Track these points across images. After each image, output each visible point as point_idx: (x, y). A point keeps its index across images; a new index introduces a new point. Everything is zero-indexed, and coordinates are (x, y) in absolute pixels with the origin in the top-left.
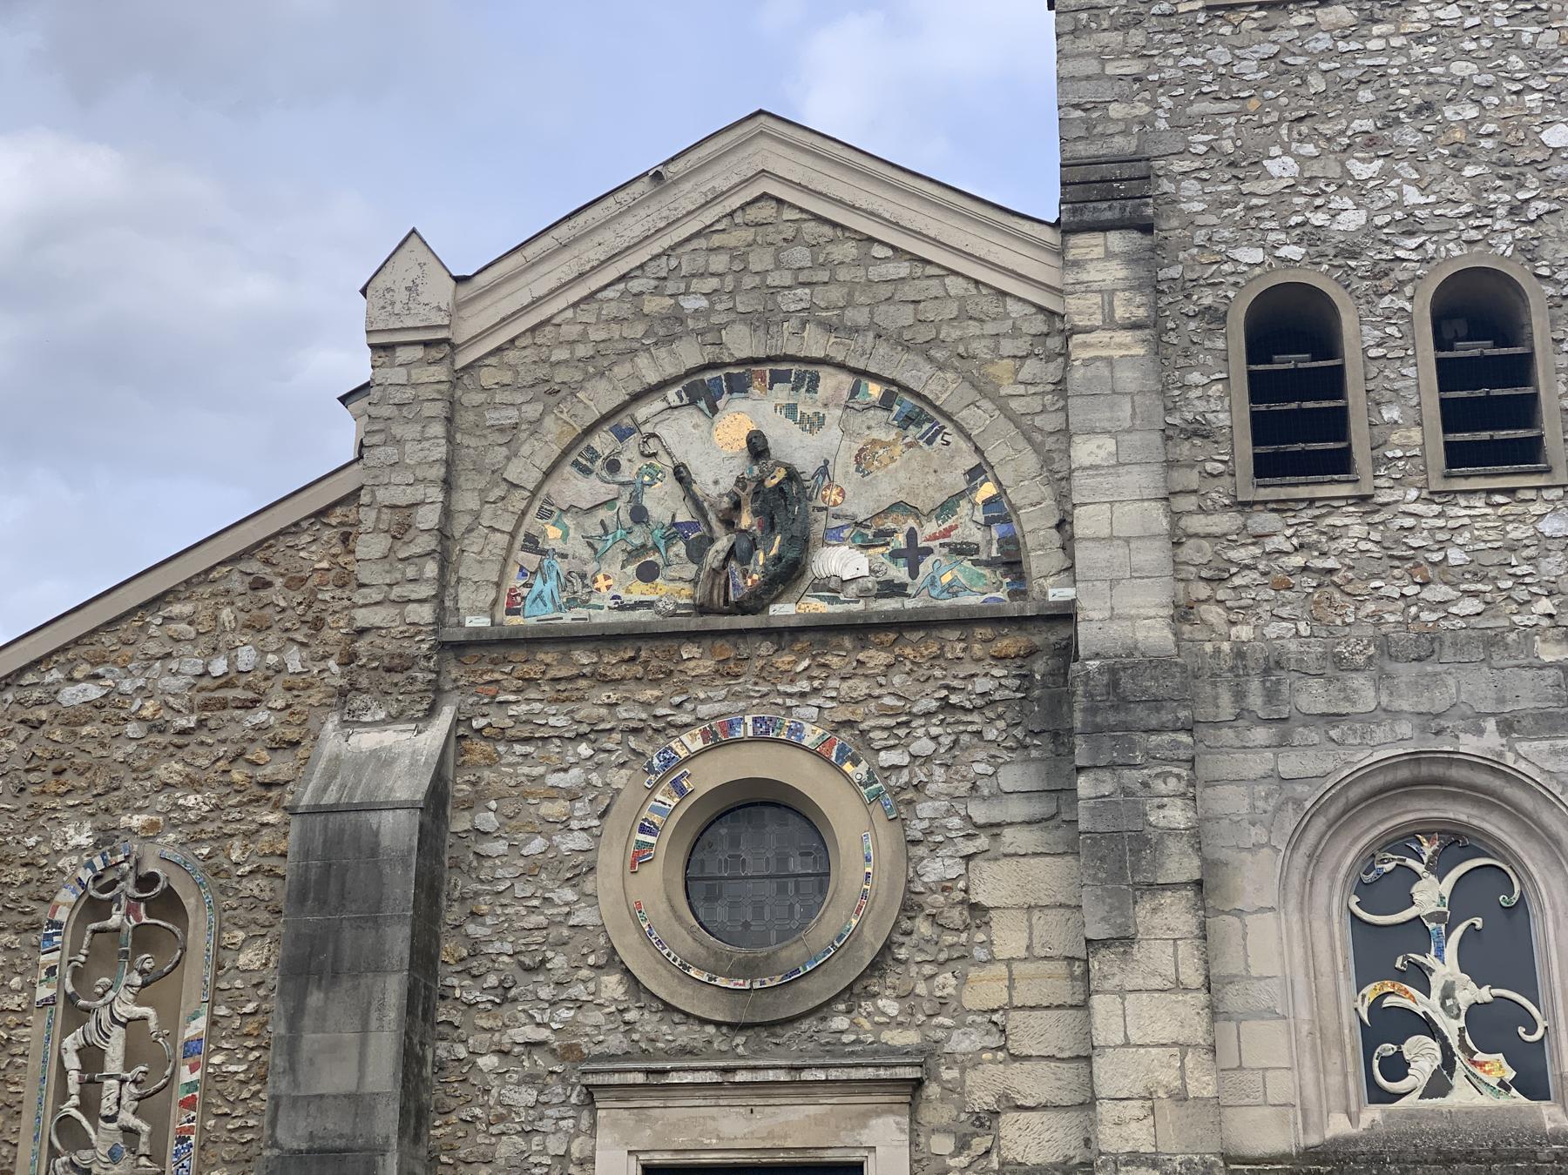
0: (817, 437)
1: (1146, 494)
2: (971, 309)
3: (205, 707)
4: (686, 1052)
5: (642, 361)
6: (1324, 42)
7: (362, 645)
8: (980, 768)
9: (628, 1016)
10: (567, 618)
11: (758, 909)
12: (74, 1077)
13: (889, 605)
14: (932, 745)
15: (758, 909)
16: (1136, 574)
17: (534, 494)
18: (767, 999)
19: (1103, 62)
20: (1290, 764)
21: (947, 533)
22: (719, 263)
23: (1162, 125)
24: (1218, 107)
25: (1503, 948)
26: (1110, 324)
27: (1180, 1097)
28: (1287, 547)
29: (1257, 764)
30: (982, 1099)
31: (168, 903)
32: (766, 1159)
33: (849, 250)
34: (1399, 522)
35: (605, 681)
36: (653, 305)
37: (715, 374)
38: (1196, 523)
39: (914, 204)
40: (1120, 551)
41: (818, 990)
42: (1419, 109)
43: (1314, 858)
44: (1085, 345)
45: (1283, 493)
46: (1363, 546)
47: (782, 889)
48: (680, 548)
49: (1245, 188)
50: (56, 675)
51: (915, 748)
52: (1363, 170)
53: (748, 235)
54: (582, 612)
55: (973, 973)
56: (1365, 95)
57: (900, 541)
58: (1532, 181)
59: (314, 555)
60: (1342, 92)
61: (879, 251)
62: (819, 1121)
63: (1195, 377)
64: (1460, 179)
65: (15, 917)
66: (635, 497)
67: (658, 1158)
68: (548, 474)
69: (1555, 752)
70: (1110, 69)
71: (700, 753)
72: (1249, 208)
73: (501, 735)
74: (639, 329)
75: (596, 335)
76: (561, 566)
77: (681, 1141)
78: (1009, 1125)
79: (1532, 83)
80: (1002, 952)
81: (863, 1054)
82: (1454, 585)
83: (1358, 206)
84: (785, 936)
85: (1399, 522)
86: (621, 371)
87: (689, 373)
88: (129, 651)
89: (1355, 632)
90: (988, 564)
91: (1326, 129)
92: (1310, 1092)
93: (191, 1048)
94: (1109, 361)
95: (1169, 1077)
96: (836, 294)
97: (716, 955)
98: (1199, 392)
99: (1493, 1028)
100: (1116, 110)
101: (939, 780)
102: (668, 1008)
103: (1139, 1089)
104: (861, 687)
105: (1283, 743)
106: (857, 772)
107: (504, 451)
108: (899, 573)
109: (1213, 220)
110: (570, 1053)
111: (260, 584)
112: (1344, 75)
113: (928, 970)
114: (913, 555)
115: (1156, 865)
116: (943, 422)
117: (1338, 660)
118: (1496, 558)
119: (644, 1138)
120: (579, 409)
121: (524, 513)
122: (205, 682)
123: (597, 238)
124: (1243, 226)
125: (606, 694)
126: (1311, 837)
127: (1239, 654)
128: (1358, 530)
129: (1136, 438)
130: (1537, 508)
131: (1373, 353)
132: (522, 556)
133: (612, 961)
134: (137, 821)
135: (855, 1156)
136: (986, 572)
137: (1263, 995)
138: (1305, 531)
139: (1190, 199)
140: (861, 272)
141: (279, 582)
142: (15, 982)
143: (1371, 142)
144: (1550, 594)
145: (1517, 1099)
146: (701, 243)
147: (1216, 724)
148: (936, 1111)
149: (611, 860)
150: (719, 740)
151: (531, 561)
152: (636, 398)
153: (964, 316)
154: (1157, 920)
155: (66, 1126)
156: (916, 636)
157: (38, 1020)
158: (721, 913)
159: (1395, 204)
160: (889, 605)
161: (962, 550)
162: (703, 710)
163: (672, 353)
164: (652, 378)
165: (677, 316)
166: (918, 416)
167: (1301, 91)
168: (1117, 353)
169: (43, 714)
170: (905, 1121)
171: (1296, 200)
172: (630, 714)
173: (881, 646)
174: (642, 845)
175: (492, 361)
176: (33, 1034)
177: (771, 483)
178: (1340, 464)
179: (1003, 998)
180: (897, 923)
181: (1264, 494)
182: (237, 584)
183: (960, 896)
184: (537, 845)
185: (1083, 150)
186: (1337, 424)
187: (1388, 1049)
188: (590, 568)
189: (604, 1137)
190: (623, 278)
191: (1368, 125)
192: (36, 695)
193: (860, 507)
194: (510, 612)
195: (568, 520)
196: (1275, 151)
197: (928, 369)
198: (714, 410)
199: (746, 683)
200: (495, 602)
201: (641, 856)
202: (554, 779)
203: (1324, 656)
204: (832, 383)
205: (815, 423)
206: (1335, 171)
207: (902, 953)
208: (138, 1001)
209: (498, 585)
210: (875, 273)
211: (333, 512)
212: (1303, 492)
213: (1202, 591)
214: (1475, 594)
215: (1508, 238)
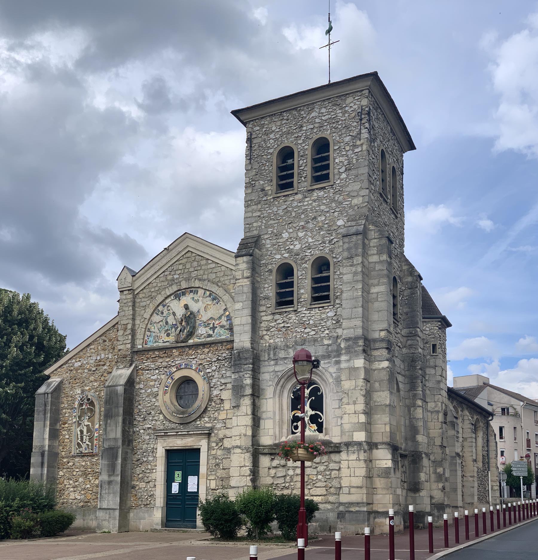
0: (197, 304)
1: (248, 315)
2: (226, 273)
3: (97, 366)
4: (173, 429)
5: (167, 290)
6: (295, 204)
7: (119, 353)
8: (224, 372)
9: (164, 422)
10: (155, 345)
11: (188, 402)
12: (79, 435)
13: (209, 339)
14: (215, 368)
15: (188, 402)
16: (245, 332)
17: (149, 320)
18: (186, 419)
19: (253, 213)
20: (277, 368)
21: (220, 323)
22: (181, 267)
23: (263, 227)
24: (274, 222)
25: (318, 404)
26: (243, 278)
27: (245, 435)
28: (281, 322)
29: (271, 369)
30: (221, 436)
31: (92, 403)
32: (184, 448)
33: (204, 262)
34: (301, 315)
35: (160, 357)
36: (169, 277)
37: (180, 292)
38: (264, 318)
39: (214, 251)
40: (242, 327)
41: (194, 417)
42: (313, 219)
43: (283, 387)
44: (238, 283)
45: (280, 311)
46: (295, 321)
47: (192, 397)
48: (174, 329)
49: (278, 241)
50: (74, 361)
51: (213, 368)
52: (301, 234)
53: (185, 260)
54: (157, 344)
55: (221, 412)
56: (303, 216)
57: (211, 326)
58: (334, 234)
59: (112, 335)
60: (298, 216)
61: (210, 262)
62: (193, 441)
63: (266, 286)
64: (320, 235)
65: (70, 407)
66: (166, 319)
67: (167, 448)
68: (151, 315)
69: (325, 363)
70: (254, 215)
71: (176, 371)
72: (279, 246)
73: (143, 369)
74: (167, 283)
75: (159, 285)
76: (154, 334)
77: (171, 445)
78: (225, 441)
79: (336, 210)
80: (225, 408)
81: (202, 428)
82: (310, 328)
83: (299, 243)
84: (189, 407)
85: (301, 315)
86: (163, 293)
87: (175, 292)
88: (85, 355)
89: (291, 340)
90: (226, 329)
91: (295, 225)
92: (277, 433)
93: (96, 430)
94: (242, 286)
95: (243, 432)
96: (201, 272)
97: (178, 410)
98: (266, 289)
99: (314, 419)
100: (255, 225)
101: (216, 375)
102: (170, 421)
103: (238, 434)
104: (203, 356)
105: (276, 364)
106: (202, 374)
107: (144, 311)
108: (211, 332)
109: (272, 249)
110: (154, 429)
111: (105, 341)
112: (299, 211)
113: (213, 412)
114: (213, 328)
115: (244, 391)
116: (220, 299)
117: (288, 347)
118: (319, 322)
119: (165, 445)
120: (156, 301)
121: (147, 324)
122: (97, 361)
123: (158, 264)
124: (277, 250)
125: (161, 360)
126: (281, 383)
127: (269, 346)
128: (294, 318)
129: (246, 303)
130: (327, 311)
131: (300, 278)
132: (147, 333)
133: (161, 413)
134: (87, 388)
135: (199, 447)
136: (226, 331)
137: (270, 415)
138: (284, 318)
139: (268, 244)
140: (206, 267)
141: (107, 340)
142: (70, 419)
143: (303, 227)
144: (328, 329)
145: (317, 433)
146: (177, 263)
147: (265, 361)
148: (213, 439)
149: (161, 393)
150: (178, 369)
151: (148, 333)
152: (166, 298)
153: (224, 275)
154: (244, 402)
155: (78, 444)
156: (213, 345)
157: (74, 425)
158: (182, 402)
159: (307, 242)
160: (209, 339)
161: (222, 327)
162: (177, 362)
163: (172, 288)
164: (168, 294)
165: (173, 280)
166: (215, 298)
167: (291, 216)
168: (244, 284)
169: (72, 368)
170: (207, 441)
171: (288, 243)
172: (165, 364)
173: (207, 348)
174: (166, 390)
175: (141, 292)
176: (73, 428)
177: (187, 315)
178: (291, 302)
179: (225, 417)
180: (208, 403)
181: (277, 311)
182: (101, 341)
183: (219, 397)
184: (149, 391)
185: (248, 234)
186: (291, 293)
187: (295, 424)
188: (158, 335)
189: (159, 445)
190: (164, 272)
191: (302, 223)
192: (71, 365)
193: (204, 319)
194: (145, 344)
195: (155, 325)
196: (284, 231)
197: (217, 287)
198: (180, 300)
199: (184, 357)
200: (143, 342)
201: (165, 392)
202: (152, 377)
203: (285, 346)
204: (201, 292)
205: (197, 301)
206: (295, 236)
207: (209, 409)
208: (88, 422)
209: (143, 339)
210: (209, 266)
211: (114, 326)
212: (284, 310)
213: (265, 333)
214: (314, 330)
215: (328, 248)
